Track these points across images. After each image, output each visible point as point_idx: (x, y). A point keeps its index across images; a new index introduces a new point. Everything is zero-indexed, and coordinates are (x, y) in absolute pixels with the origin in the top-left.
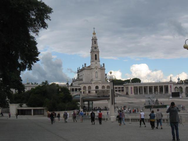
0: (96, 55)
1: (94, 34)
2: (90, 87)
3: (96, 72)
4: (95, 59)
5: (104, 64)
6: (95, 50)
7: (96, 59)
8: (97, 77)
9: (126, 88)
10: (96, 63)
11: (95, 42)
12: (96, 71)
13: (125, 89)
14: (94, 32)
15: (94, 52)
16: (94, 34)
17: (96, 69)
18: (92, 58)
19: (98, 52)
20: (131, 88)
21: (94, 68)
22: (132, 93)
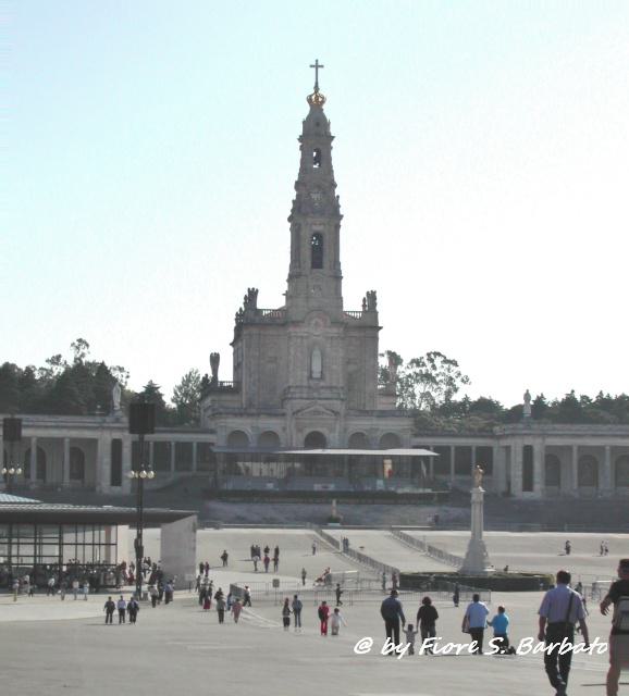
1: (316, 103)
4: (309, 263)
7: (317, 263)
8: (316, 375)
13: (498, 458)
16: (316, 103)
20: (528, 451)
22: (528, 485)
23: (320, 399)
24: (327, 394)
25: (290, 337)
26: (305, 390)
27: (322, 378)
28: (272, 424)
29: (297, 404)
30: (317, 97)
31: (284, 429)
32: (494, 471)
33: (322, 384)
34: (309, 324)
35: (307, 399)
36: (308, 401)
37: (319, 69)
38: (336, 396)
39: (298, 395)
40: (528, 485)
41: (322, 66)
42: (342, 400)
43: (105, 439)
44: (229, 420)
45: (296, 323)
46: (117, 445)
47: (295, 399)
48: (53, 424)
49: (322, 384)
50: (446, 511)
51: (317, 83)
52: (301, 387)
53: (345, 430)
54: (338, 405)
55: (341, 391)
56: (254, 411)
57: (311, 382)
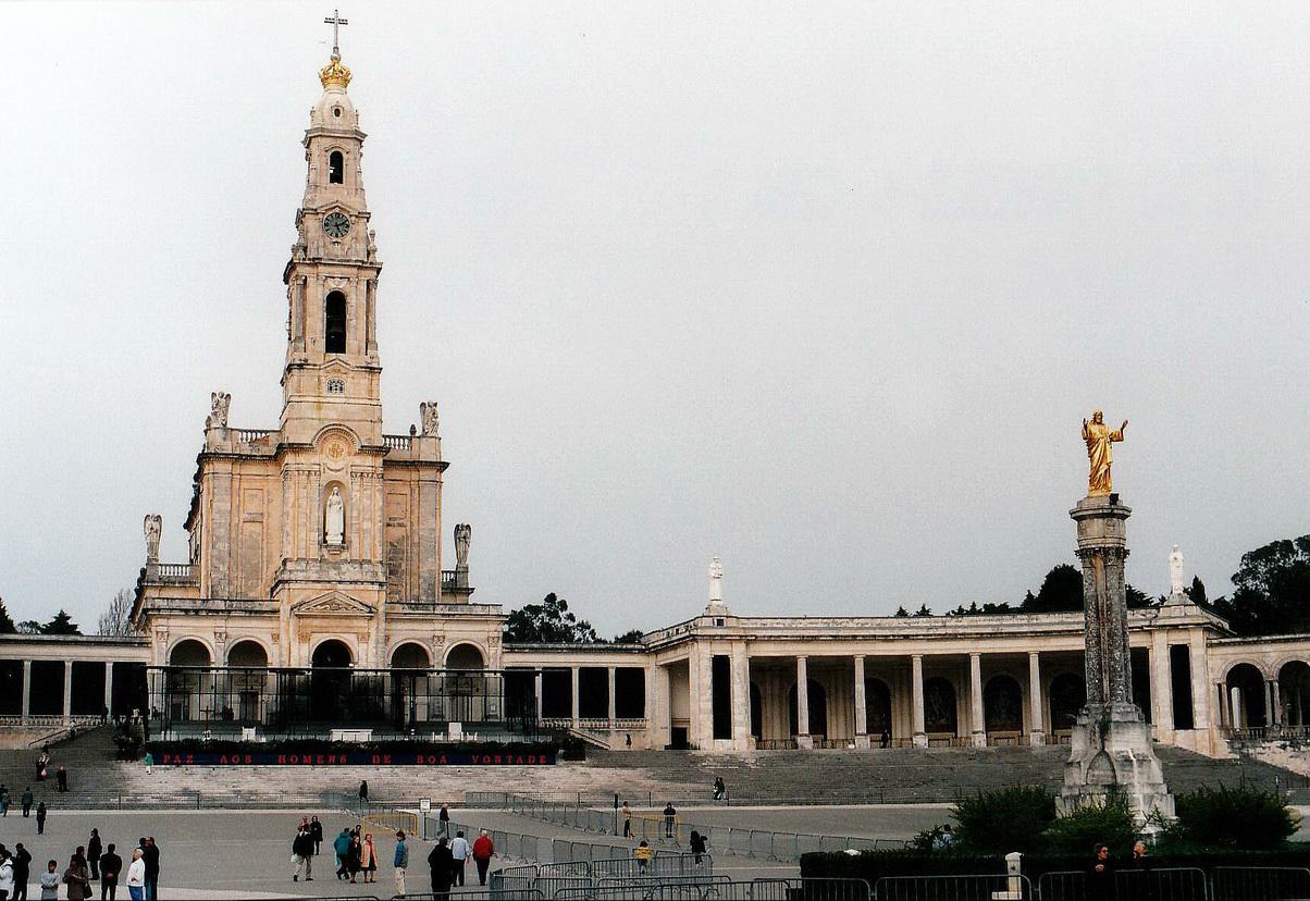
0: (336, 303)
1: (336, 75)
2: (248, 653)
3: (331, 485)
4: (322, 343)
5: (428, 409)
6: (320, 245)
7: (336, 342)
8: (334, 538)
9: (664, 678)
10: (336, 386)
11: (337, 160)
12: (325, 479)
13: (656, 687)
14: (336, 60)
15: (316, 262)
16: (336, 75)
17: (335, 452)
18: (296, 338)
19: (370, 267)
20: (721, 666)
21: (305, 439)
22: (722, 729)
23: (340, 582)
24: (351, 572)
27: (345, 544)
31: (276, 637)
33: (345, 555)
35: (319, 582)
36: (319, 586)
39: (301, 576)
40: (722, 729)
41: (344, 22)
42: (381, 584)
44: (172, 622)
45: (297, 448)
51: (336, 48)
53: (387, 638)
56: (221, 605)
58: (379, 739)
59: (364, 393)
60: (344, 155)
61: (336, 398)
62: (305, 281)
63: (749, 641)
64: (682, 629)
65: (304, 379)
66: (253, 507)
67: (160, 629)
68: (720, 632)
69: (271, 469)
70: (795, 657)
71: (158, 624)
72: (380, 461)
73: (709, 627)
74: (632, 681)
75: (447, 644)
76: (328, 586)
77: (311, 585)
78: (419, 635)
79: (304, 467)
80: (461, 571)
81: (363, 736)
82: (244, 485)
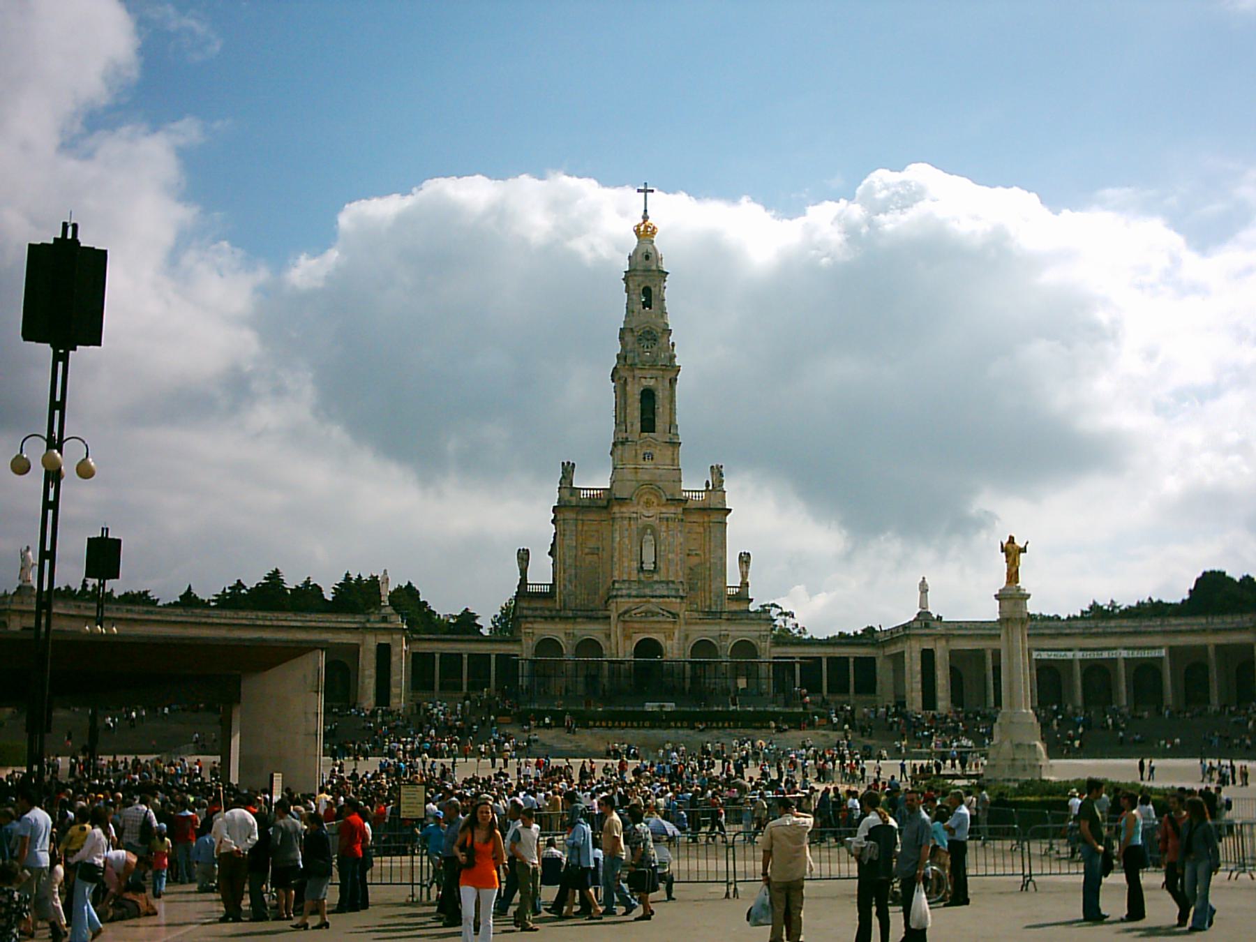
0: (648, 396)
3: (645, 528)
4: (638, 426)
7: (648, 424)
11: (647, 292)
13: (884, 672)
14: (645, 218)
17: (648, 504)
18: (621, 421)
19: (671, 370)
20: (928, 657)
25: (613, 519)
26: (634, 586)
27: (655, 570)
28: (594, 631)
29: (624, 604)
30: (646, 227)
31: (608, 636)
32: (878, 687)
33: (656, 577)
34: (638, 504)
35: (637, 597)
36: (638, 600)
37: (648, 194)
38: (673, 593)
39: (624, 592)
42: (682, 598)
43: (371, 642)
44: (536, 626)
45: (622, 501)
46: (384, 652)
47: (622, 596)
48: (299, 624)
49: (656, 577)
50: (827, 736)
51: (646, 211)
52: (630, 582)
53: (687, 637)
54: (675, 605)
55: (680, 587)
56: (570, 614)
57: (641, 575)
58: (679, 709)
59: (668, 461)
60: (653, 289)
61: (648, 464)
62: (626, 379)
63: (947, 637)
64: (901, 629)
65: (628, 451)
66: (592, 543)
67: (528, 631)
68: (927, 631)
69: (604, 515)
70: (983, 650)
71: (526, 628)
72: (680, 510)
73: (917, 628)
74: (867, 666)
75: (730, 640)
76: (644, 599)
77: (631, 600)
78: (712, 634)
79: (627, 515)
80: (745, 585)
81: (670, 707)
82: (585, 528)
